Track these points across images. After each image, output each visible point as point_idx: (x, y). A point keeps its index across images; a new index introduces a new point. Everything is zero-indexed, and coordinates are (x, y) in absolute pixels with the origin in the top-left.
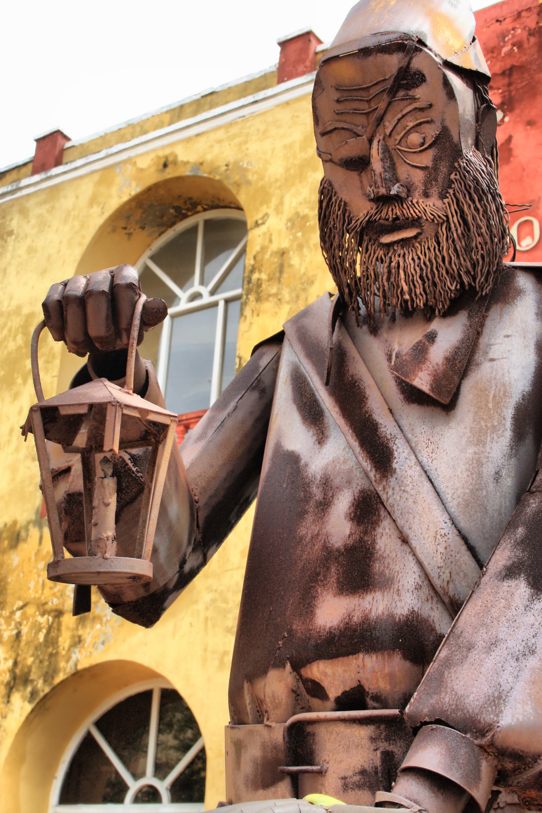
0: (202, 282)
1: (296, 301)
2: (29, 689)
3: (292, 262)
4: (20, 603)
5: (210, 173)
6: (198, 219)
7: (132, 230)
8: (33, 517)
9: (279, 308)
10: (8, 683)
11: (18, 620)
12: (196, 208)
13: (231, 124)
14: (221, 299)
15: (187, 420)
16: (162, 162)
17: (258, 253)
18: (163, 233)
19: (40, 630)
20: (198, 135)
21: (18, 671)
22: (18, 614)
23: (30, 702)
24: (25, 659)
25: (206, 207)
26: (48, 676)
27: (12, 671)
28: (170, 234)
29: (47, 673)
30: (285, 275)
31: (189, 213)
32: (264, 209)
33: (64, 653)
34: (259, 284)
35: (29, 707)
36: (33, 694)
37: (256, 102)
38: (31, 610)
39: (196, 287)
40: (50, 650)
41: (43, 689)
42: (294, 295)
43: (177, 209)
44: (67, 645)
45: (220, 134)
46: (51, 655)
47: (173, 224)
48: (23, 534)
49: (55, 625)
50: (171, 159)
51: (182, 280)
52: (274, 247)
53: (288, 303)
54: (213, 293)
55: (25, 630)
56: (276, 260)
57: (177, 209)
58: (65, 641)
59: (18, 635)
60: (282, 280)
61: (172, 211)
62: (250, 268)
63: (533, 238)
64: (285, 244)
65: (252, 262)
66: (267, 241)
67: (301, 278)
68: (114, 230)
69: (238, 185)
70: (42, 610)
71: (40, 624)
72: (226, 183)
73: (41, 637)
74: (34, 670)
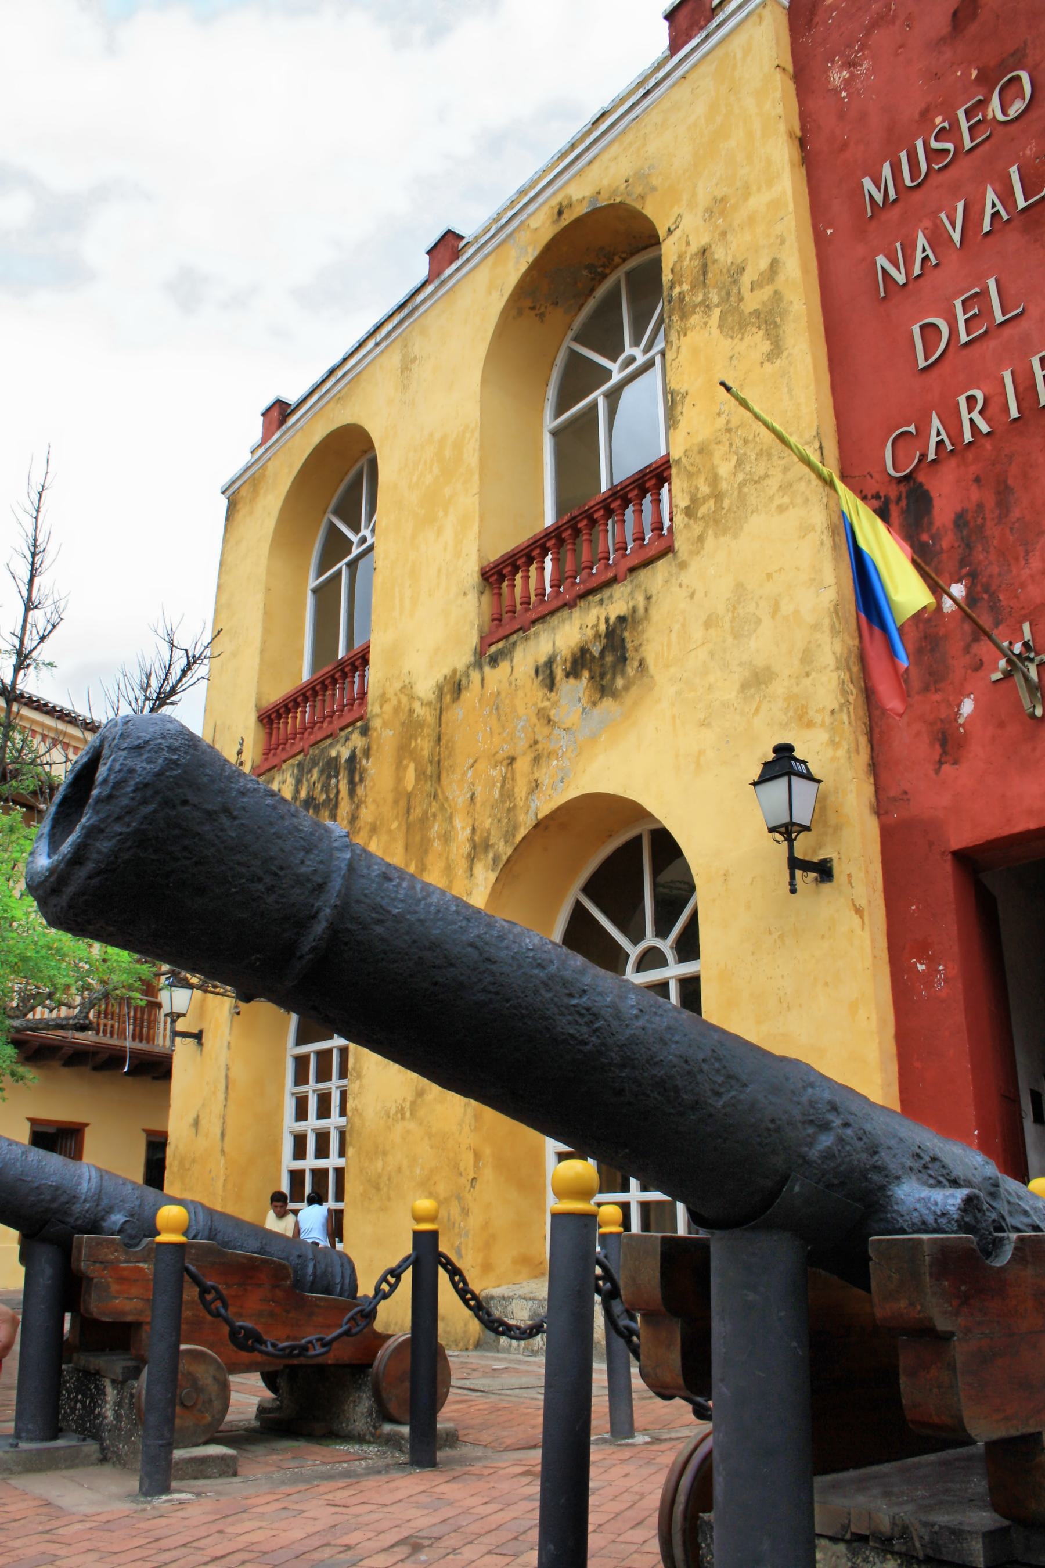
0: (636, 343)
1: (728, 300)
2: (491, 855)
3: (716, 257)
4: (471, 761)
5: (610, 199)
6: (619, 275)
7: (543, 309)
8: (472, 659)
9: (709, 316)
10: (469, 854)
11: (470, 780)
12: (613, 260)
13: (623, 132)
14: (656, 354)
15: (621, 489)
16: (556, 211)
17: (675, 263)
18: (582, 305)
19: (494, 785)
20: (590, 162)
21: (476, 838)
22: (470, 773)
23: (493, 870)
24: (483, 822)
25: (624, 255)
26: (508, 836)
27: (471, 840)
28: (591, 304)
29: (507, 831)
30: (710, 275)
31: (607, 271)
32: (676, 211)
33: (522, 804)
34: (681, 297)
35: (493, 876)
36: (496, 859)
37: (647, 93)
38: (481, 766)
39: (629, 350)
40: (507, 805)
41: (505, 851)
42: (723, 293)
43: (590, 268)
44: (524, 794)
45: (614, 149)
46: (509, 810)
47: (592, 290)
48: (464, 682)
49: (509, 775)
50: (564, 204)
51: (613, 351)
52: (694, 248)
53: (717, 306)
54: (646, 351)
55: (478, 789)
56: (696, 263)
57: (590, 268)
58: (521, 790)
59: (472, 797)
60: (707, 282)
61: (585, 273)
62: (669, 284)
63: (1024, 99)
64: (704, 240)
65: (670, 277)
66: (684, 244)
67: (729, 271)
68: (520, 312)
69: (642, 197)
70: (493, 762)
71: (494, 777)
72: (629, 201)
73: (496, 794)
74: (493, 832)
